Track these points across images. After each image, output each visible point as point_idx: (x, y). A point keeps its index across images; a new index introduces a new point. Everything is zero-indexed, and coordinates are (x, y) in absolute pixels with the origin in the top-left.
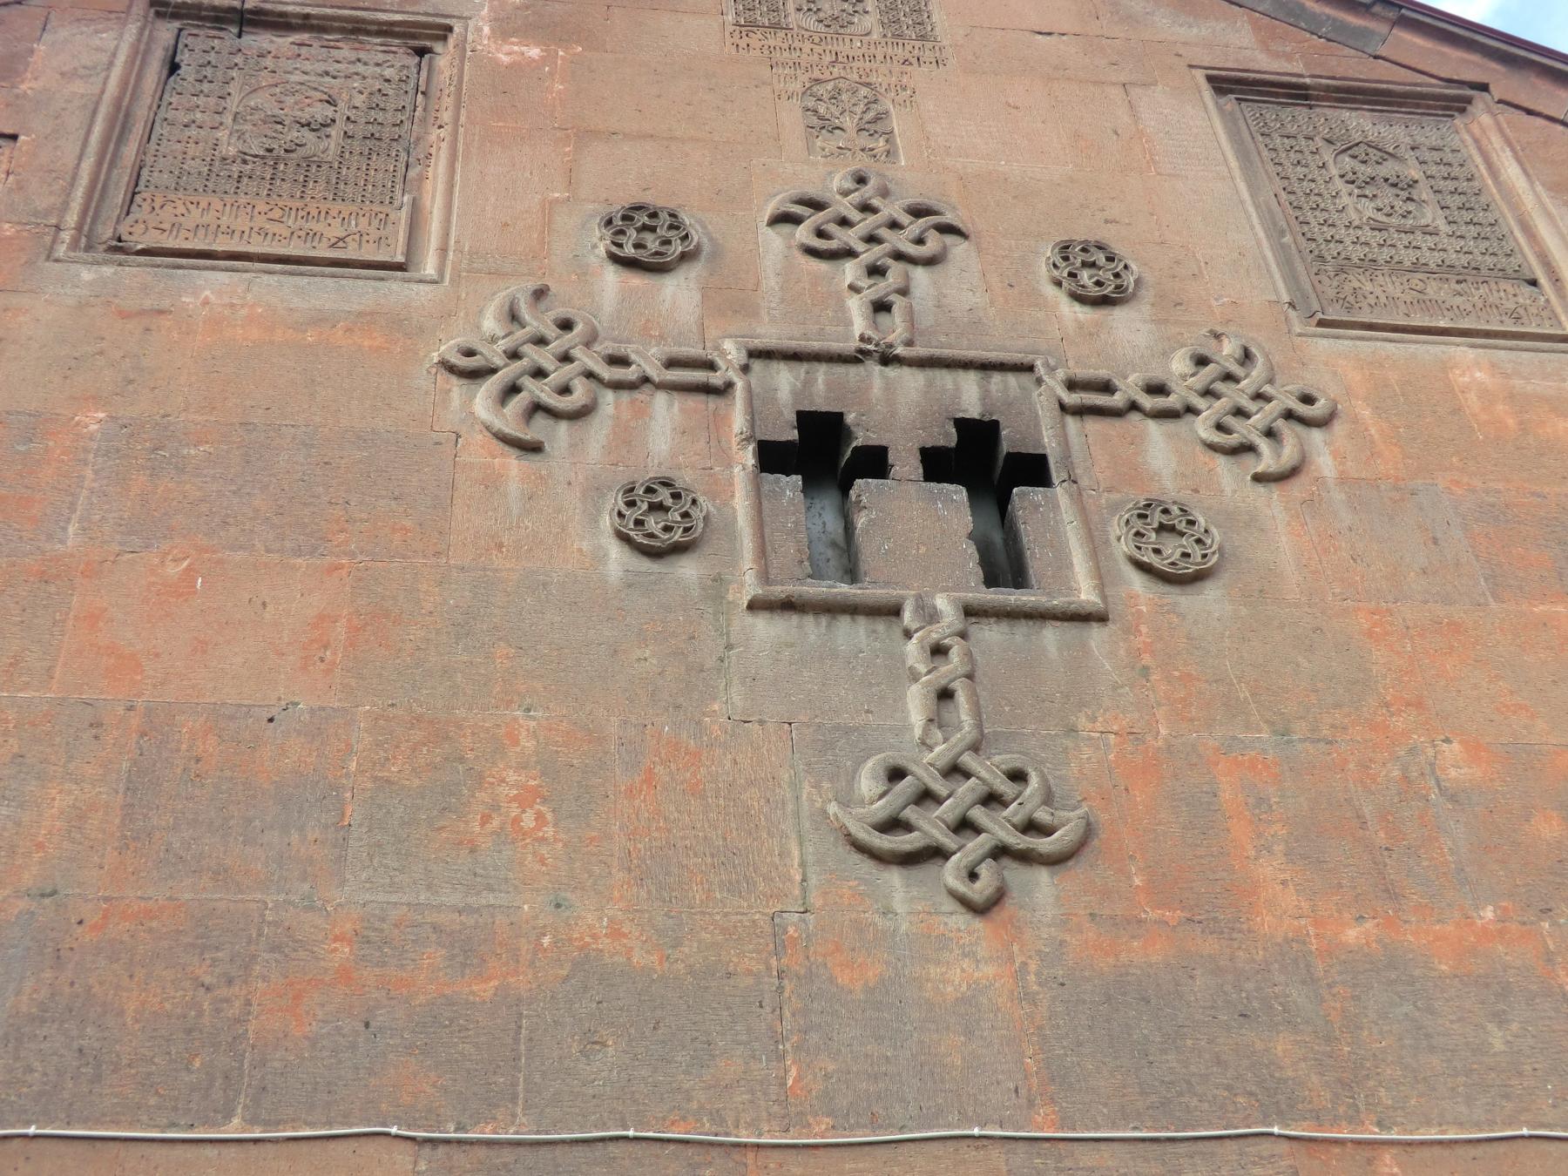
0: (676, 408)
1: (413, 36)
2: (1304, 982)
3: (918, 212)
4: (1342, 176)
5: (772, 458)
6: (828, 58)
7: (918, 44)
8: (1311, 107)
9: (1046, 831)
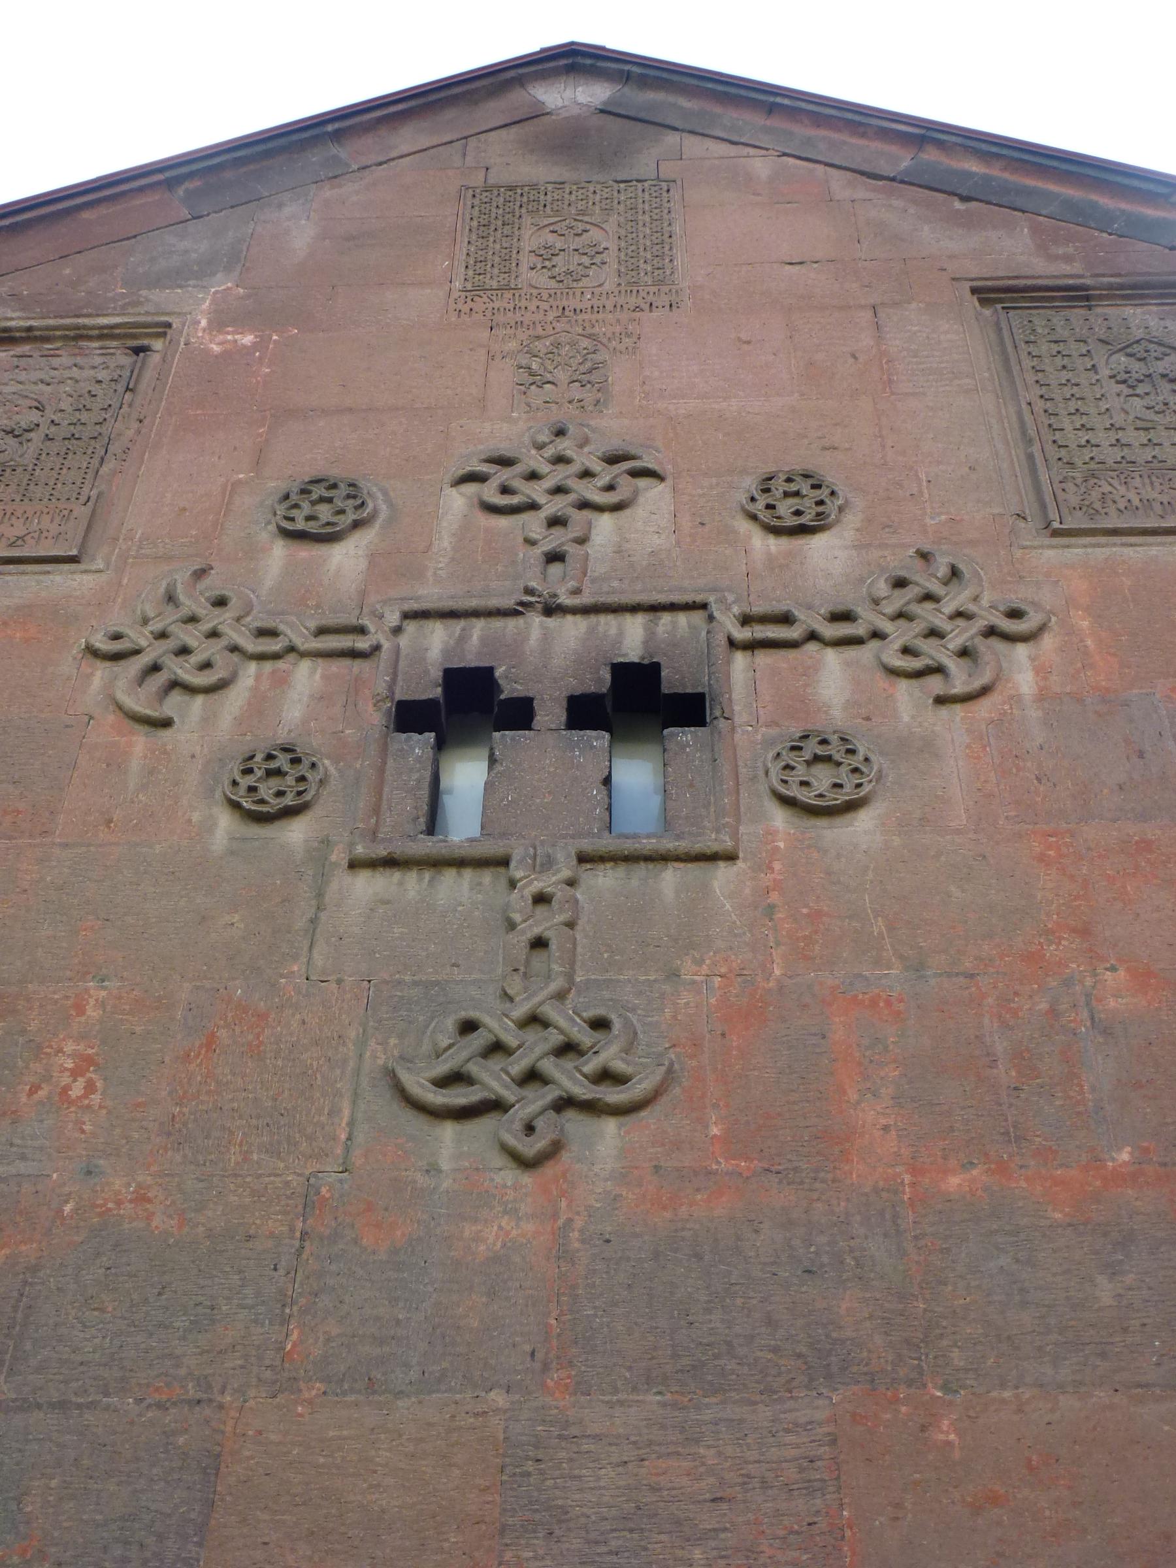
0: (317, 677)
1: (134, 337)
2: (886, 1235)
3: (612, 460)
4: (1111, 377)
5: (409, 716)
6: (551, 316)
7: (654, 289)
8: (1090, 308)
9: (619, 1079)
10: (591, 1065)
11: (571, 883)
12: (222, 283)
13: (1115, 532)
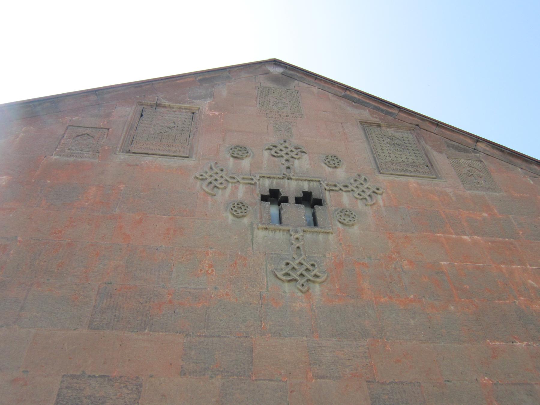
5: (264, 198)
10: (313, 273)
11: (302, 236)
12: (209, 100)
13: (392, 174)
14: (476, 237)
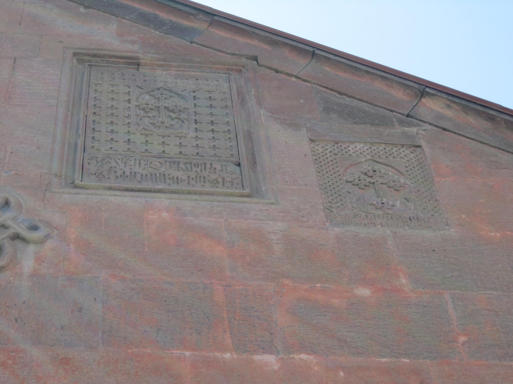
4: (136, 106)
14: (304, 356)
